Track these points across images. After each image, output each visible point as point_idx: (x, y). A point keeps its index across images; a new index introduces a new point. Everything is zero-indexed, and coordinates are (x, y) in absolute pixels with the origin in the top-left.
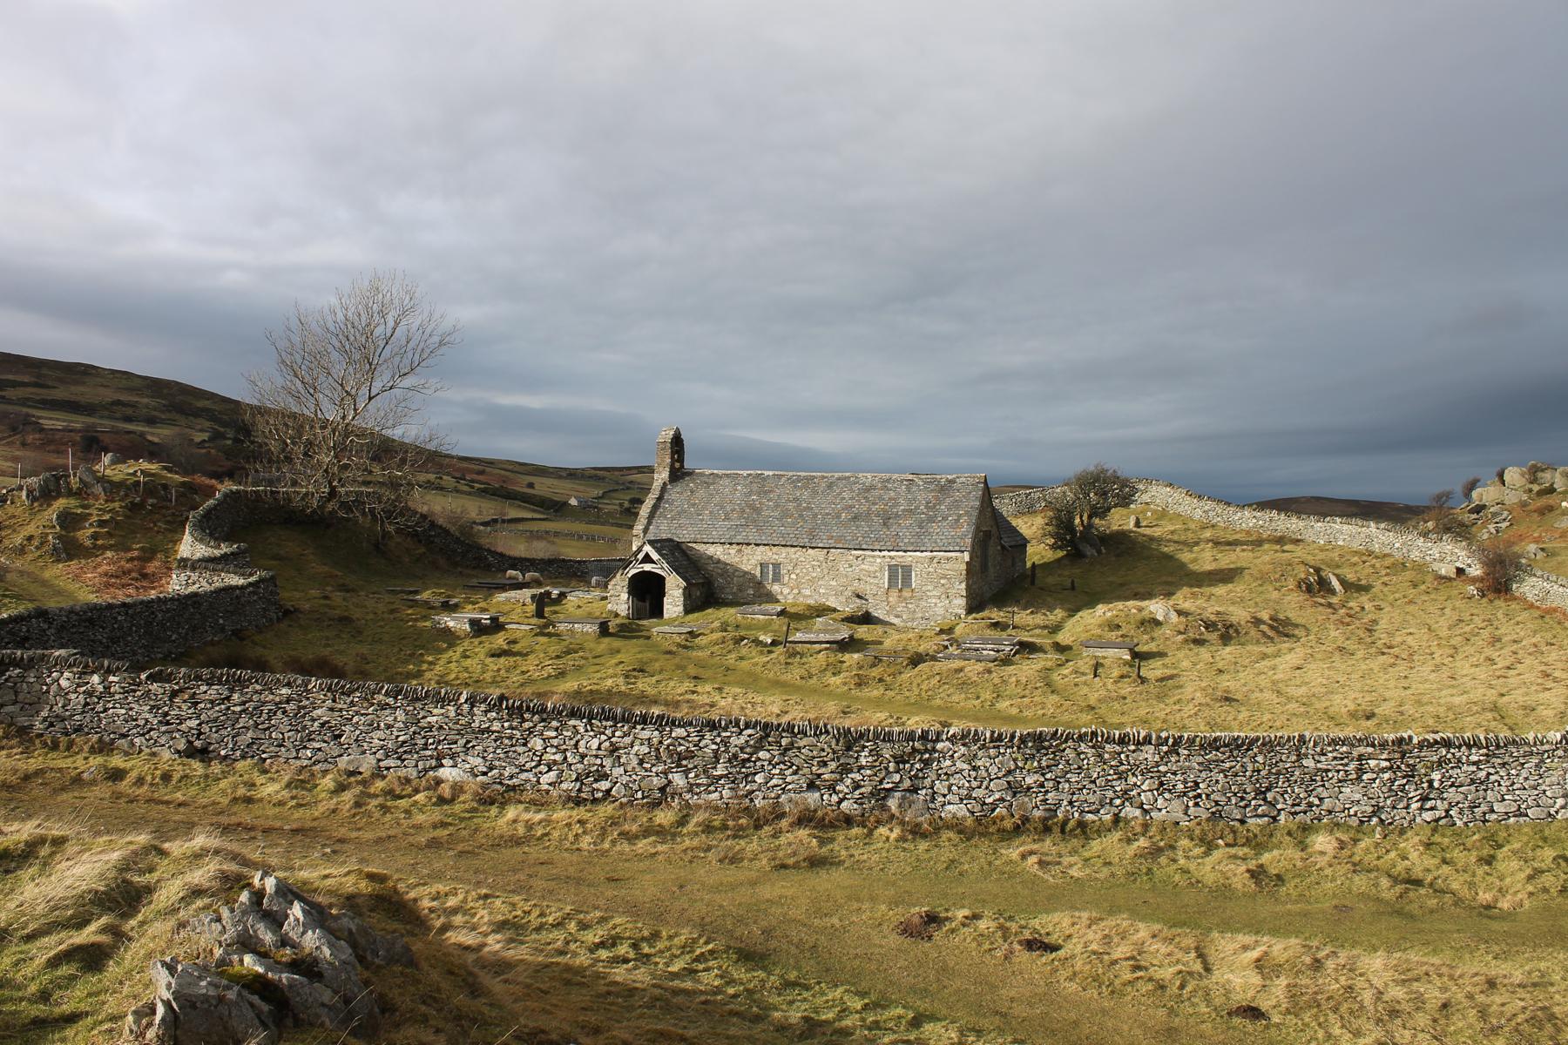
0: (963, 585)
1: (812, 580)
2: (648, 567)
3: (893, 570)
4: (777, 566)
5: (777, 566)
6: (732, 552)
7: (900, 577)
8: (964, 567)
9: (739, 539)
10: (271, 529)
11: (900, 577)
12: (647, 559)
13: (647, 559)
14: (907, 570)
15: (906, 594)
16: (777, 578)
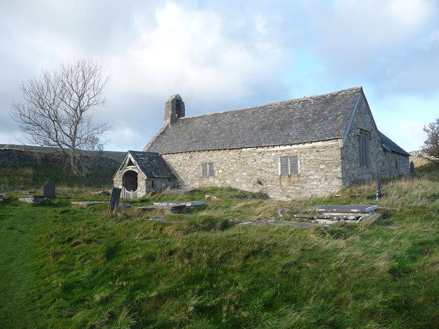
0: (339, 169)
1: (231, 174)
2: (130, 168)
3: (284, 160)
4: (211, 164)
5: (211, 164)
6: (188, 158)
7: (290, 166)
8: (339, 152)
9: (191, 149)
10: (52, 172)
11: (290, 166)
12: (130, 163)
13: (130, 163)
14: (294, 159)
15: (294, 179)
16: (212, 173)
